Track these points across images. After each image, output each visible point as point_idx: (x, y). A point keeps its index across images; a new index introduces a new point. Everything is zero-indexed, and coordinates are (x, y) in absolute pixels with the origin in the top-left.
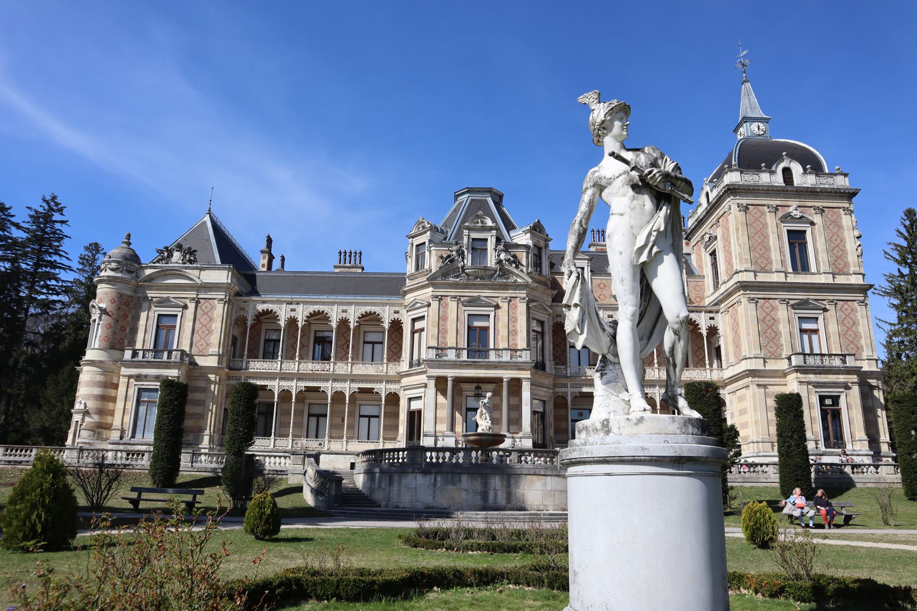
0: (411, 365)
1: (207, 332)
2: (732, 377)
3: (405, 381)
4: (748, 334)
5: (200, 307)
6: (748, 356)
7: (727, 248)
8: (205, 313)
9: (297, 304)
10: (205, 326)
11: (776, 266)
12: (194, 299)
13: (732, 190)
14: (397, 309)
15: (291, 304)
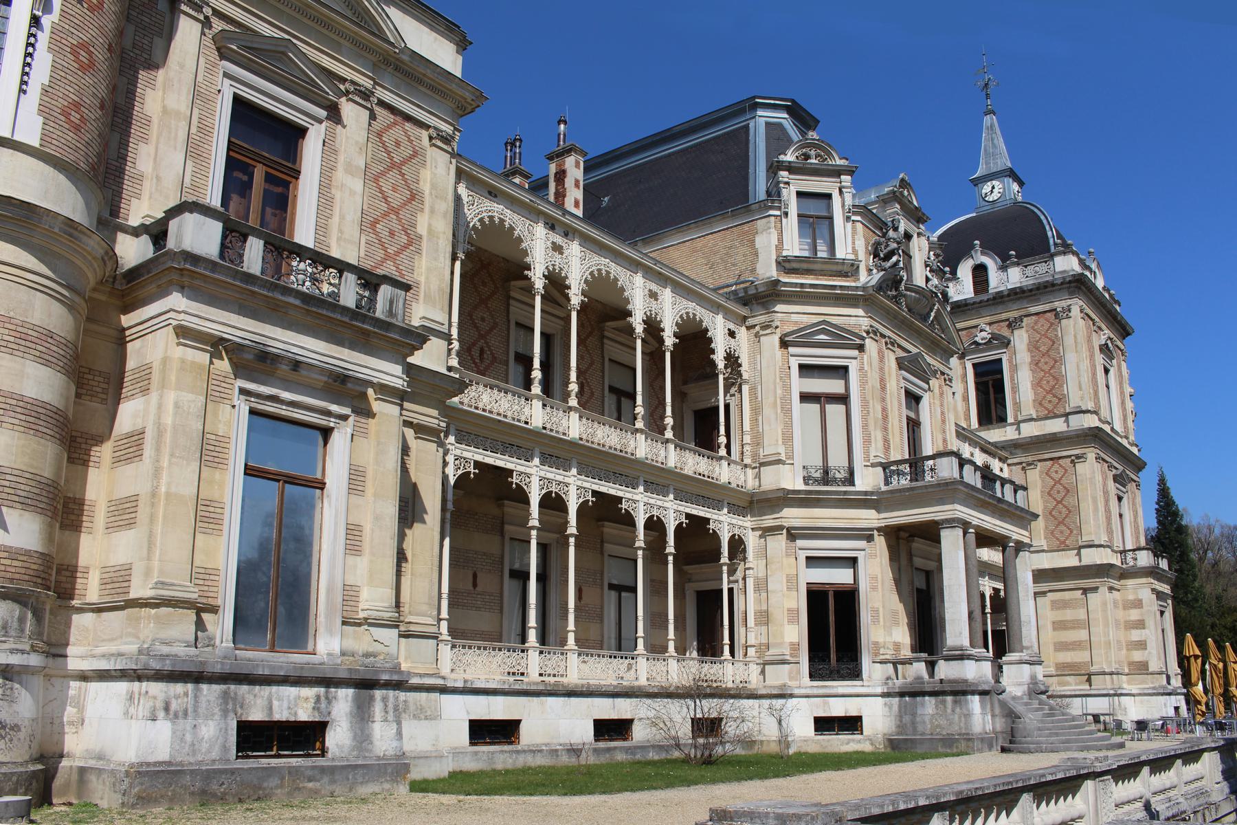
0: (806, 480)
1: (404, 239)
2: (1053, 570)
3: (793, 516)
4: (1096, 509)
5: (379, 135)
6: (1096, 543)
7: (1046, 368)
8: (393, 166)
9: (566, 235)
10: (397, 214)
11: (1104, 413)
12: (366, 95)
13: (1078, 285)
14: (732, 326)
15: (552, 228)
